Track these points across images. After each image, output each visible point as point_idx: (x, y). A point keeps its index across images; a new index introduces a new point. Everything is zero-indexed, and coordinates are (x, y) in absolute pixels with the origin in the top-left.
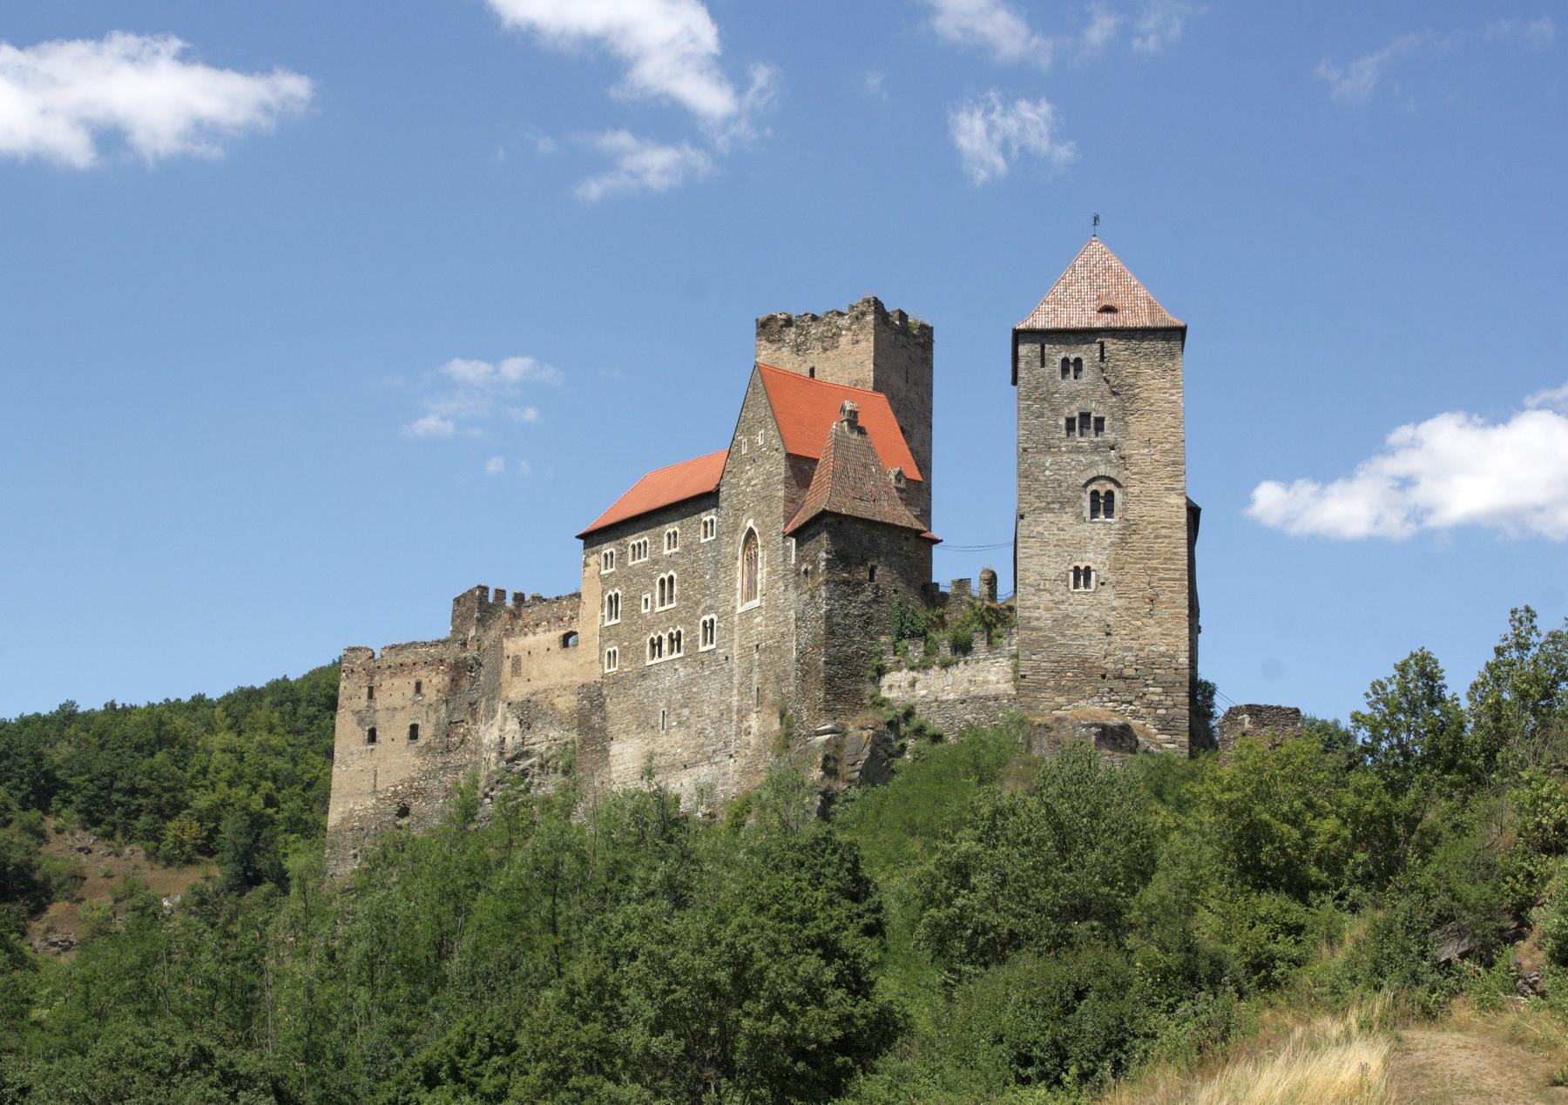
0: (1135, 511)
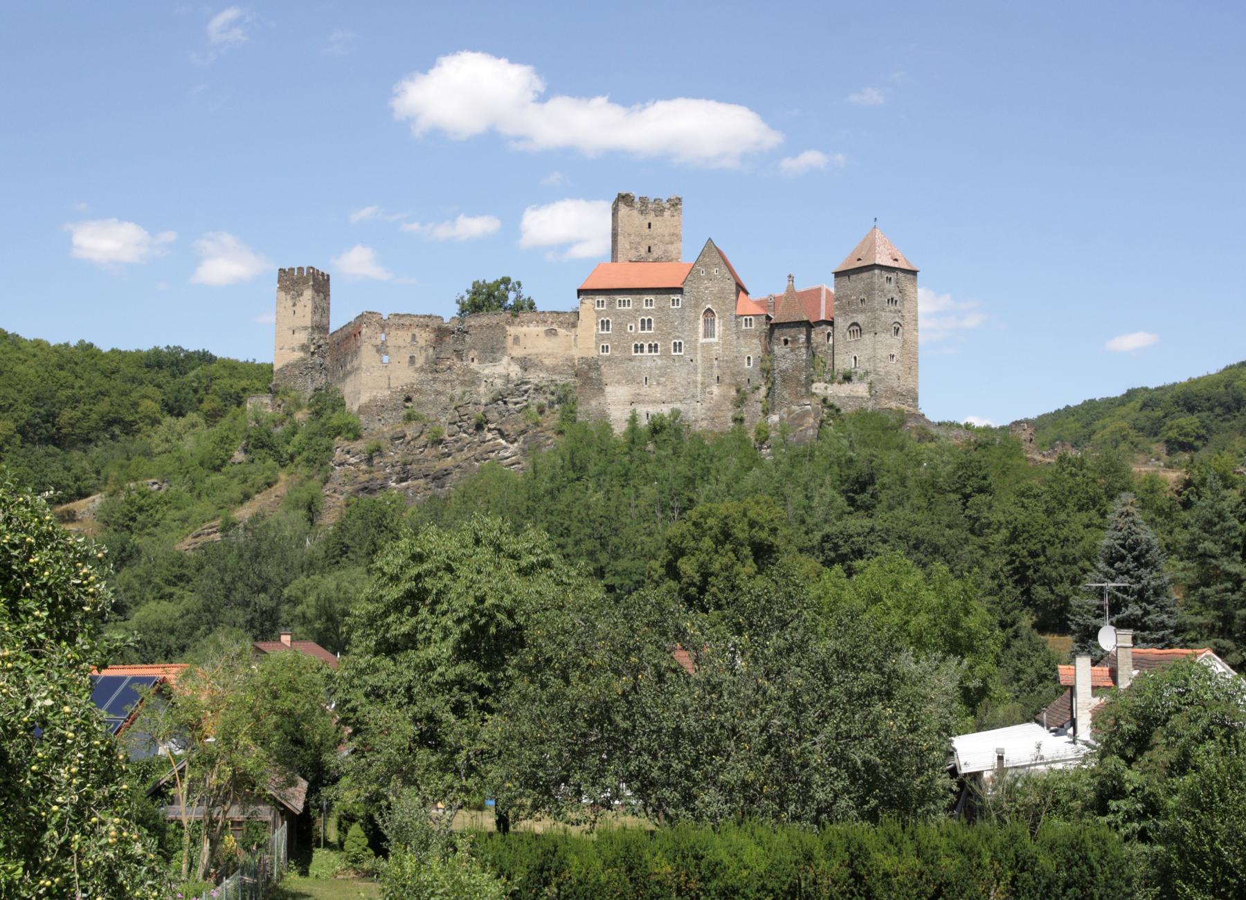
0: (907, 336)
